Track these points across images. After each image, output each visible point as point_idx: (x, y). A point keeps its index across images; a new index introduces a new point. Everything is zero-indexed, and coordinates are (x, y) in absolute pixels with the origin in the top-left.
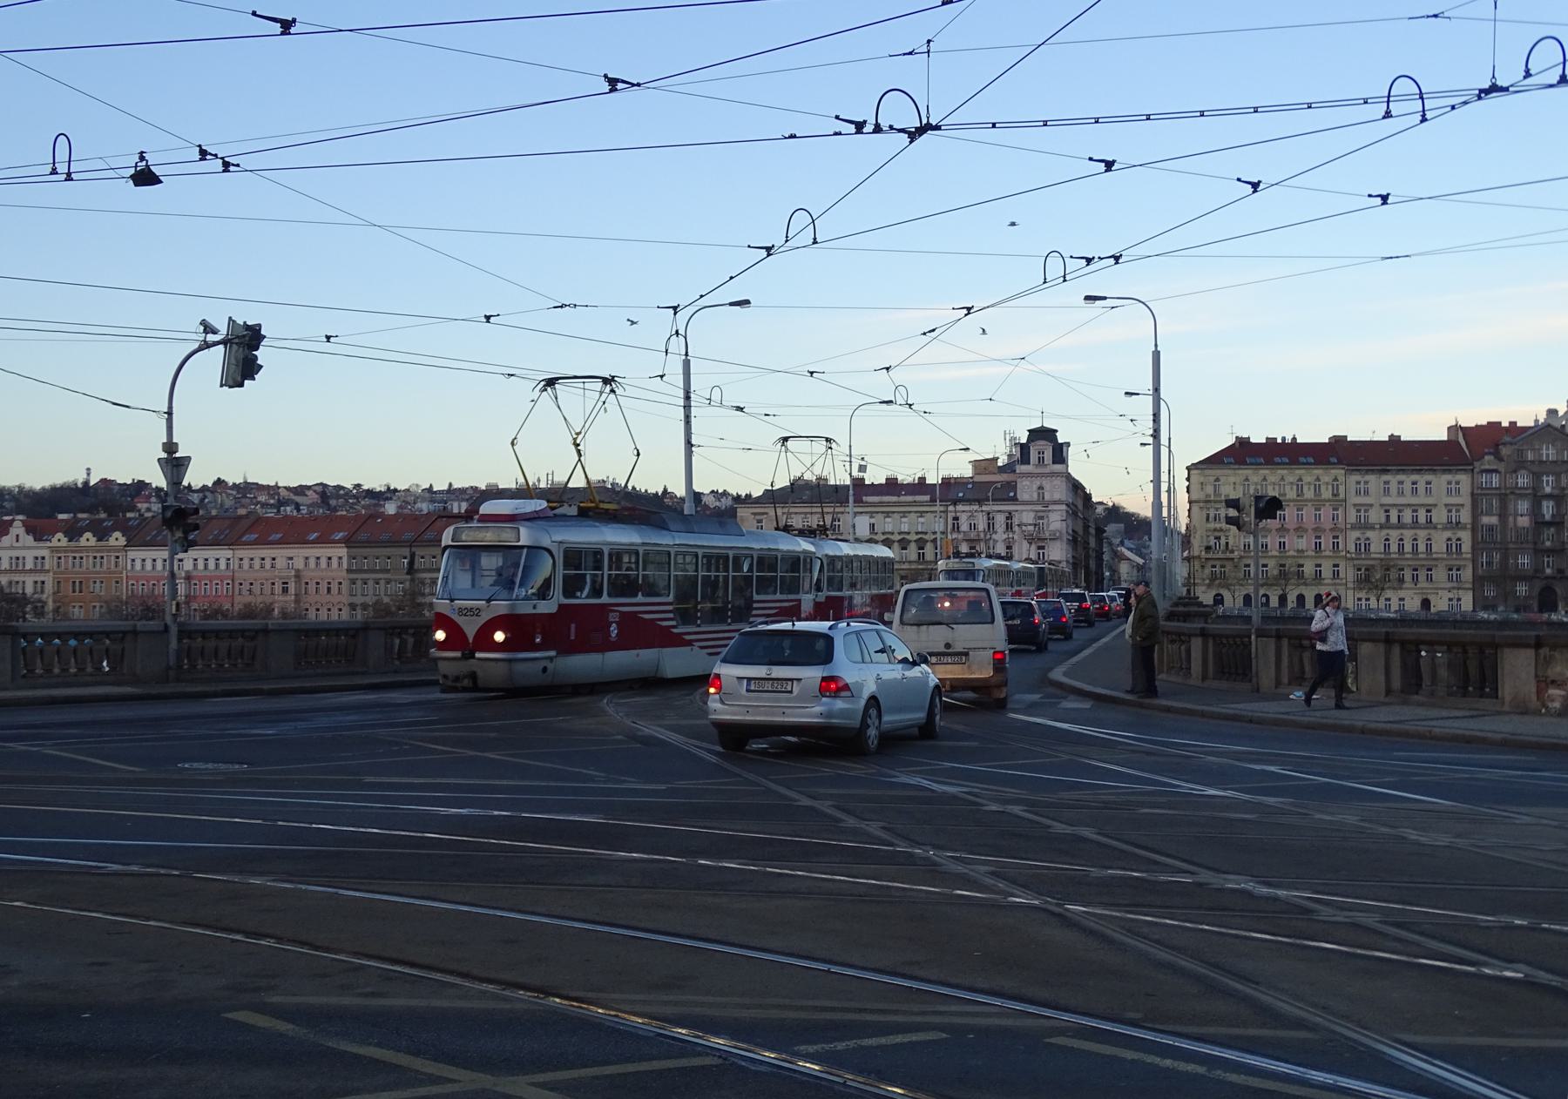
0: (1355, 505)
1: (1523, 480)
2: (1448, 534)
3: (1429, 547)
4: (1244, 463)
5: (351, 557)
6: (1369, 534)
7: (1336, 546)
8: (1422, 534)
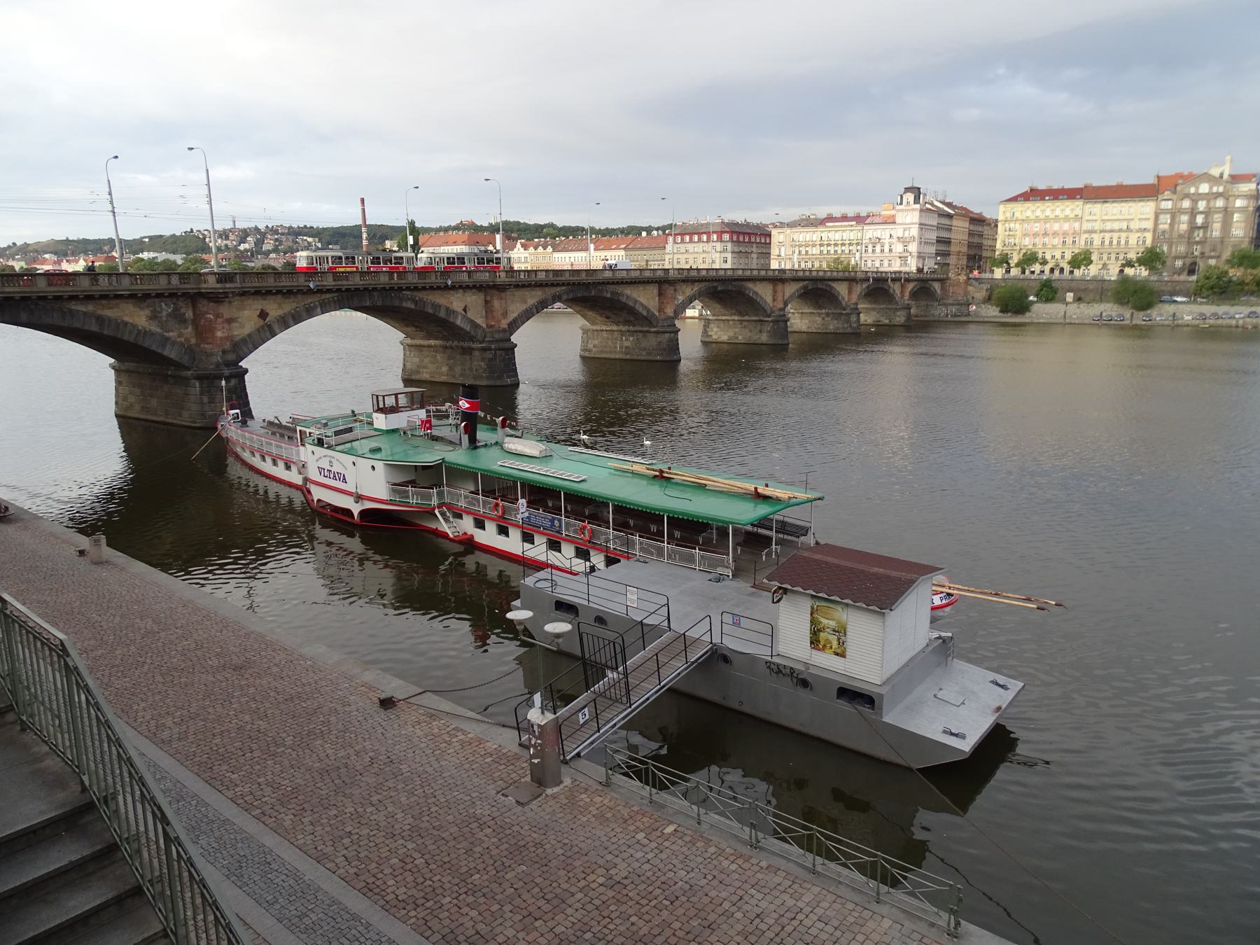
0: (1087, 221)
1: (1186, 204)
2: (1139, 234)
3: (1127, 242)
4: (1029, 200)
5: (626, 255)
6: (1094, 236)
7: (1074, 242)
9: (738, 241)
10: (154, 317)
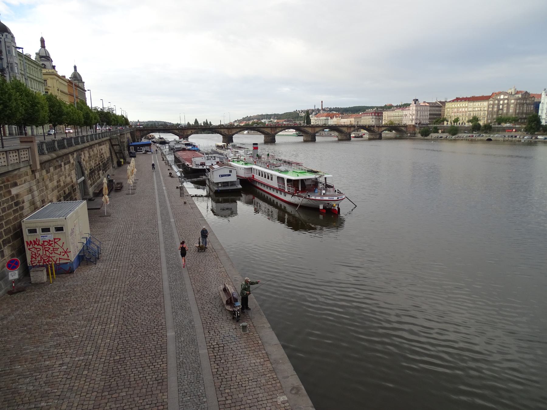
2: (483, 112)
3: (480, 114)
6: (471, 112)
8: (479, 112)
9: (378, 115)
10: (178, 131)
